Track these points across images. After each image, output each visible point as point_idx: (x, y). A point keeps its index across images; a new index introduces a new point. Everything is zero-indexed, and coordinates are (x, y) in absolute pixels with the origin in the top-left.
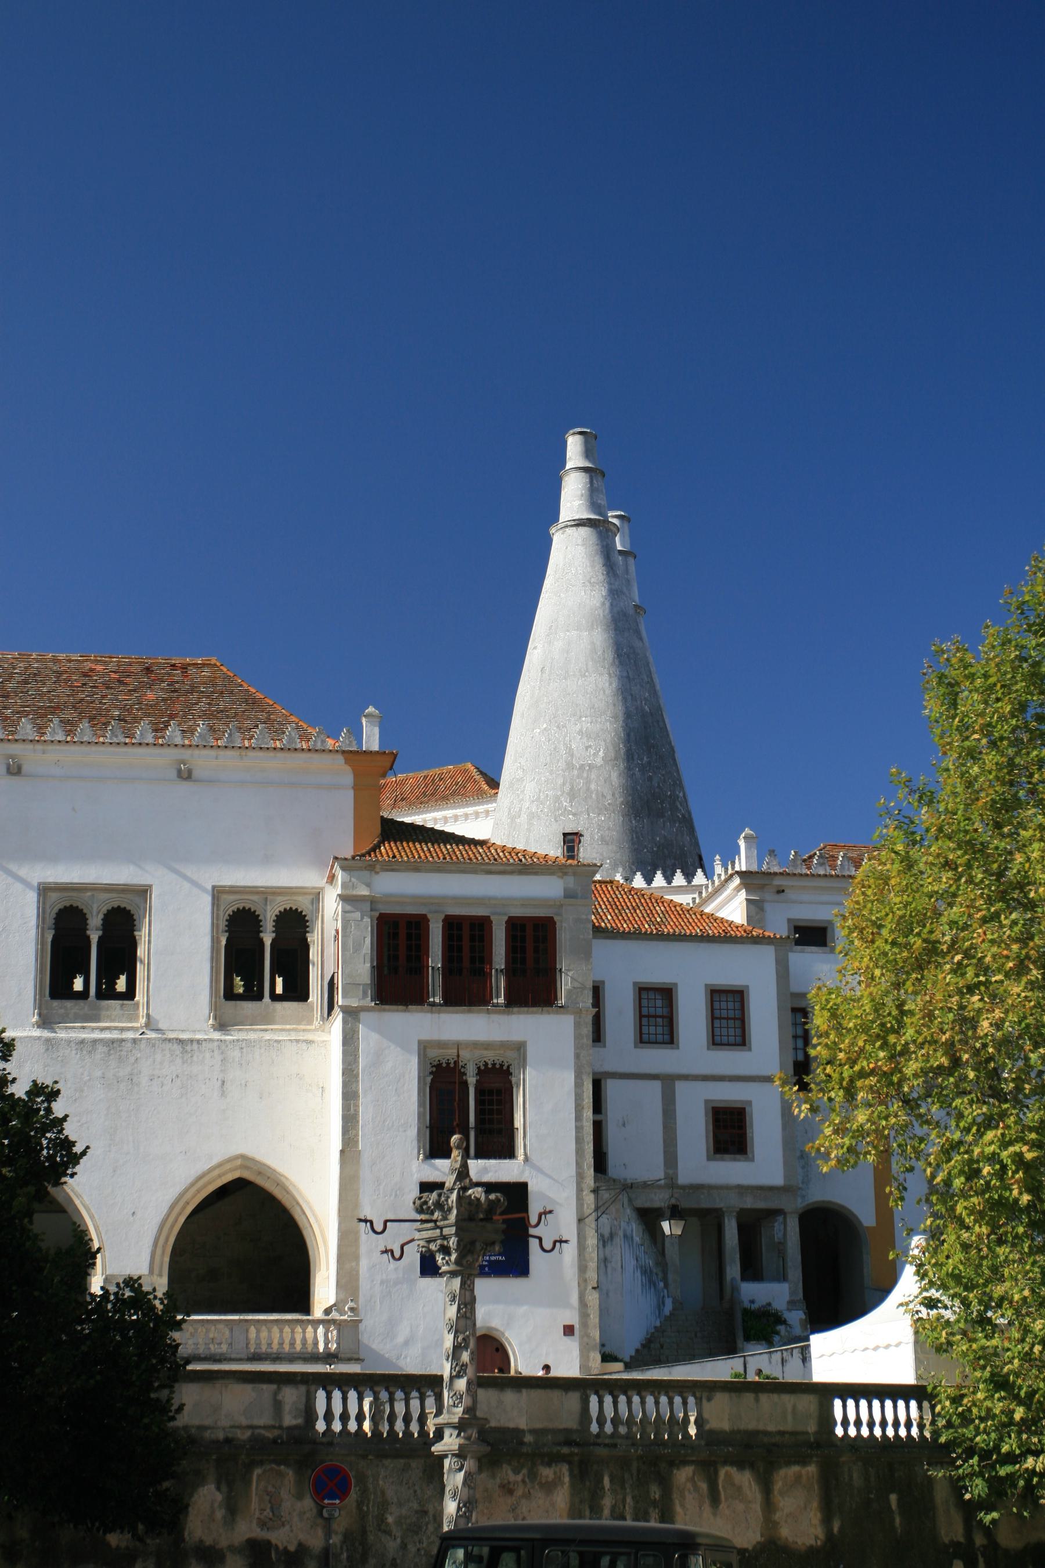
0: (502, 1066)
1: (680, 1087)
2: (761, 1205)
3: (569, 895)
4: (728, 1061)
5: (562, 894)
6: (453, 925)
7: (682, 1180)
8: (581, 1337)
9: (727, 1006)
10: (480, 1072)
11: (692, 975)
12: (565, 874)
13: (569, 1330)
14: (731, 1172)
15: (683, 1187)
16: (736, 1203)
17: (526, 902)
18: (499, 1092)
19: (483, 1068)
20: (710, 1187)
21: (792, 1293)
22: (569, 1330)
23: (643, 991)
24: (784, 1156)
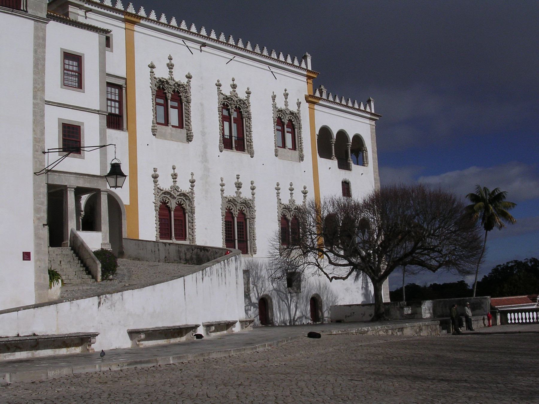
4: (71, 96)
8: (36, 261)
9: (73, 65)
13: (27, 256)
16: (73, 183)
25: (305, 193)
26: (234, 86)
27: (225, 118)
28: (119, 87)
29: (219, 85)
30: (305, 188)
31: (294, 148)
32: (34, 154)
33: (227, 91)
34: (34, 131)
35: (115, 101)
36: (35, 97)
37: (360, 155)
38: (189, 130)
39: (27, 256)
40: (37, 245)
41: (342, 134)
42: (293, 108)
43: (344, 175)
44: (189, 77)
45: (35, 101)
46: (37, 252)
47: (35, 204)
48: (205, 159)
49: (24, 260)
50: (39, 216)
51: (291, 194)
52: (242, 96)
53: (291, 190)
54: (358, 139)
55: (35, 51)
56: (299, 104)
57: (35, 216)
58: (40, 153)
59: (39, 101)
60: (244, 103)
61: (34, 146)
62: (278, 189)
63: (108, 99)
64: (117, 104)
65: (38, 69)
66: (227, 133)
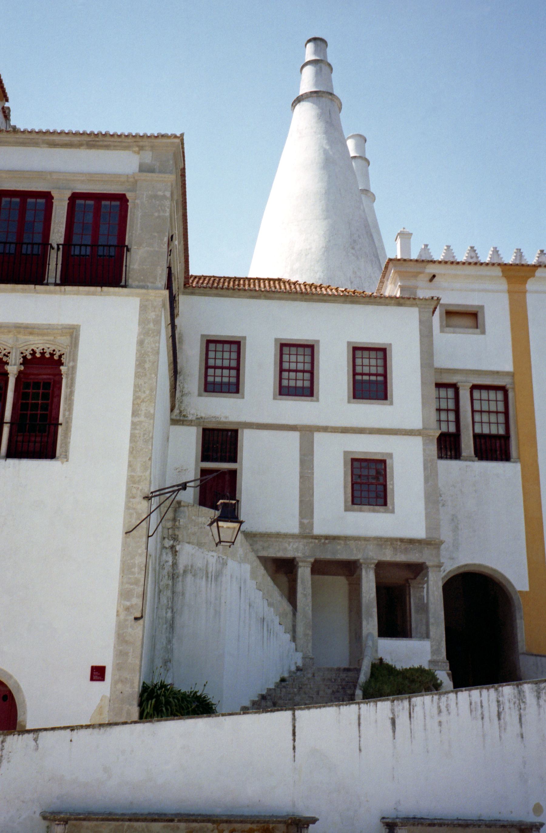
0: (52, 355)
1: (317, 436)
2: (401, 558)
3: (143, 169)
4: (369, 413)
5: (137, 170)
7: (317, 530)
8: (115, 683)
10: (25, 361)
11: (335, 333)
12: (142, 148)
14: (370, 523)
15: (318, 537)
17: (91, 177)
18: (47, 385)
19: (29, 357)
20: (346, 538)
21: (434, 652)
22: (98, 673)
23: (284, 347)
24: (426, 509)
28: (503, 389)
32: (128, 502)
34: (130, 465)
35: (497, 412)
36: (135, 413)
39: (98, 673)
45: (136, 419)
46: (119, 667)
47: (122, 583)
49: (92, 679)
50: (128, 604)
55: (141, 343)
57: (119, 603)
58: (139, 499)
59: (142, 418)
61: (129, 490)
63: (439, 410)
64: (501, 418)
65: (145, 369)
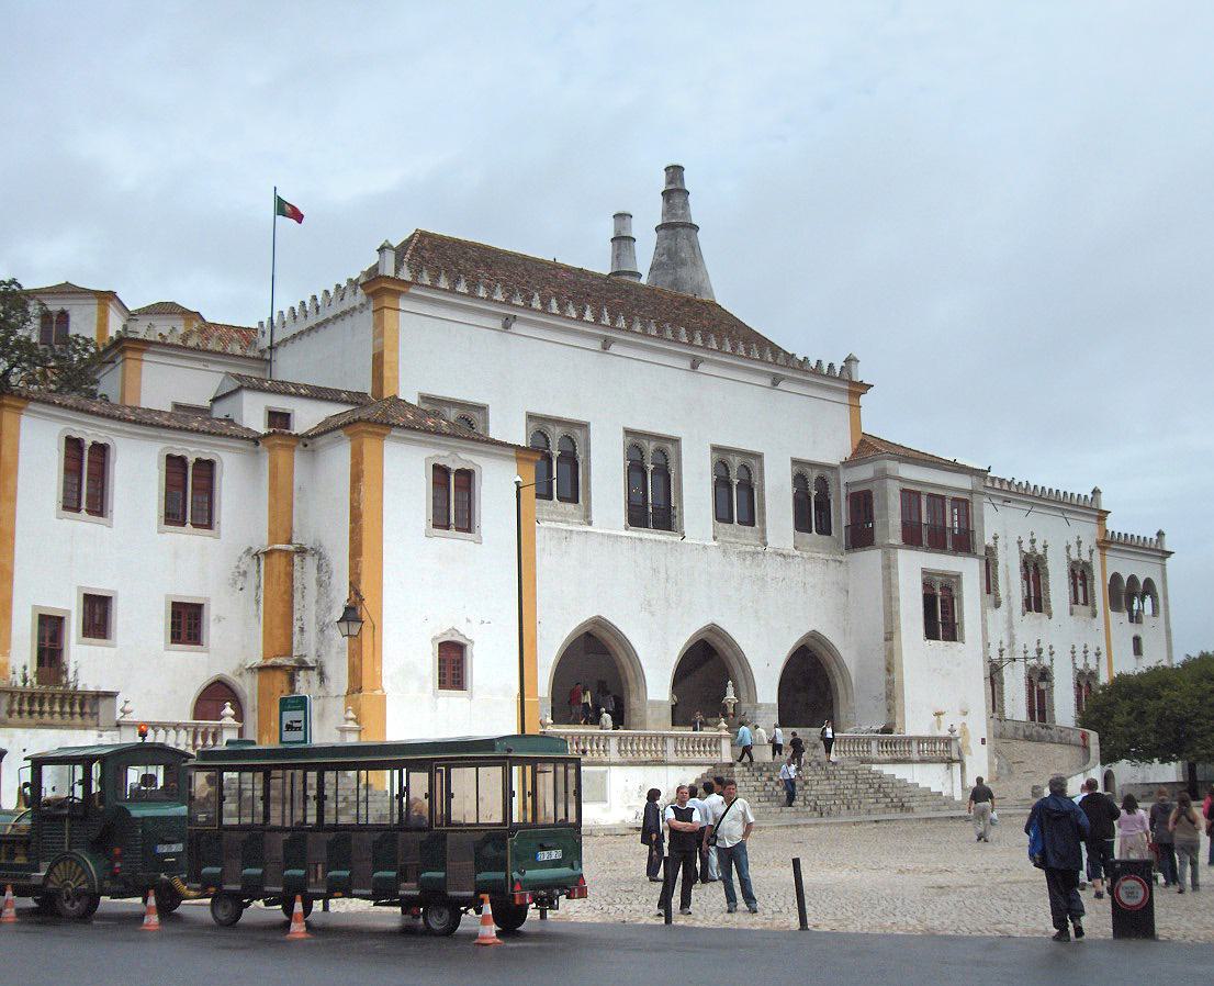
6: (930, 495)
25: (1098, 655)
26: (1033, 541)
27: (1026, 577)
29: (1020, 543)
30: (1098, 649)
31: (1086, 603)
33: (1027, 548)
37: (1148, 600)
38: (997, 595)
39: (983, 741)
40: (988, 732)
41: (1132, 579)
42: (1085, 557)
43: (1133, 630)
44: (995, 538)
46: (989, 738)
48: (1011, 626)
51: (1086, 657)
52: (1040, 551)
53: (1086, 652)
54: (1148, 582)
56: (1091, 552)
60: (1042, 559)
62: (1073, 653)
66: (1026, 592)
